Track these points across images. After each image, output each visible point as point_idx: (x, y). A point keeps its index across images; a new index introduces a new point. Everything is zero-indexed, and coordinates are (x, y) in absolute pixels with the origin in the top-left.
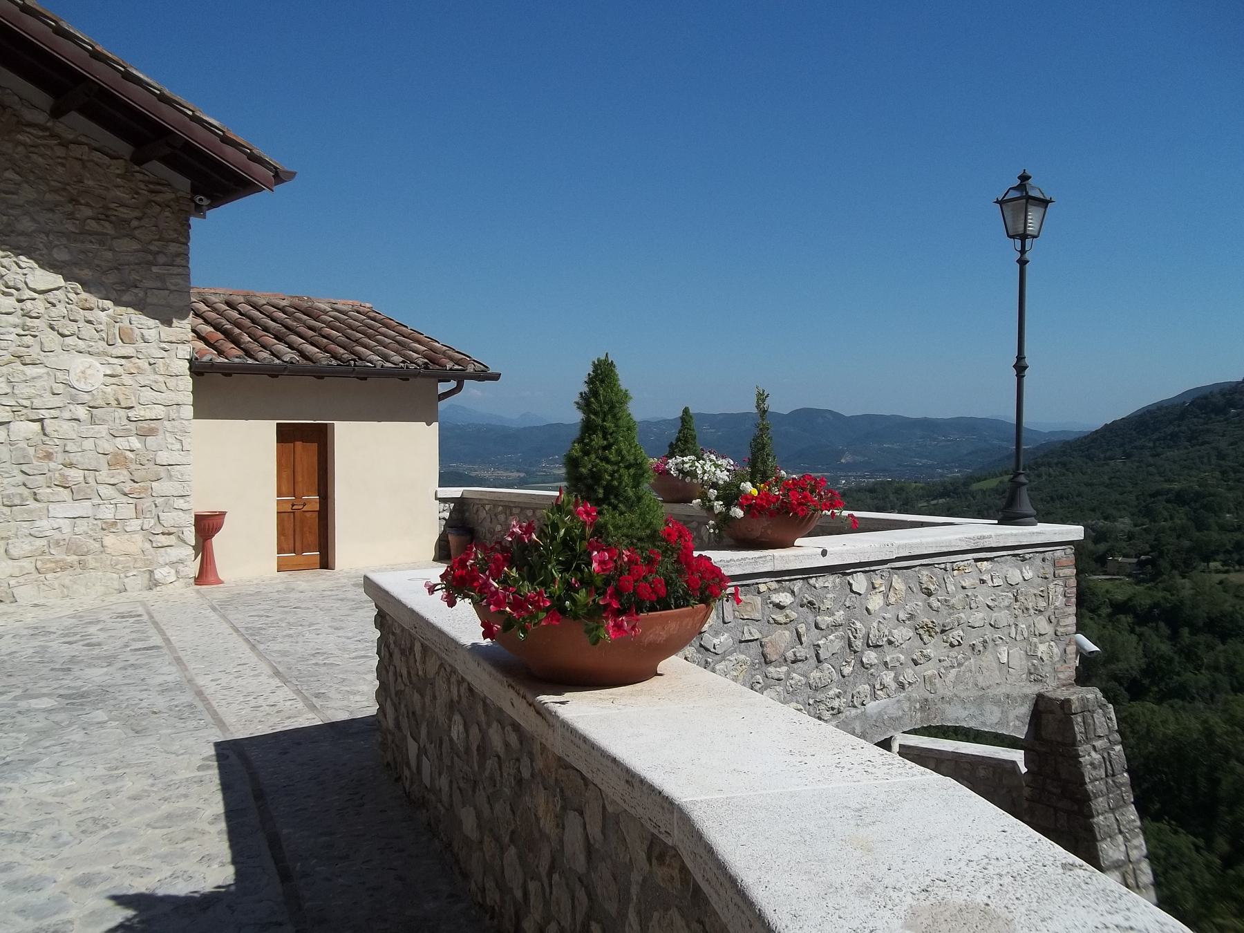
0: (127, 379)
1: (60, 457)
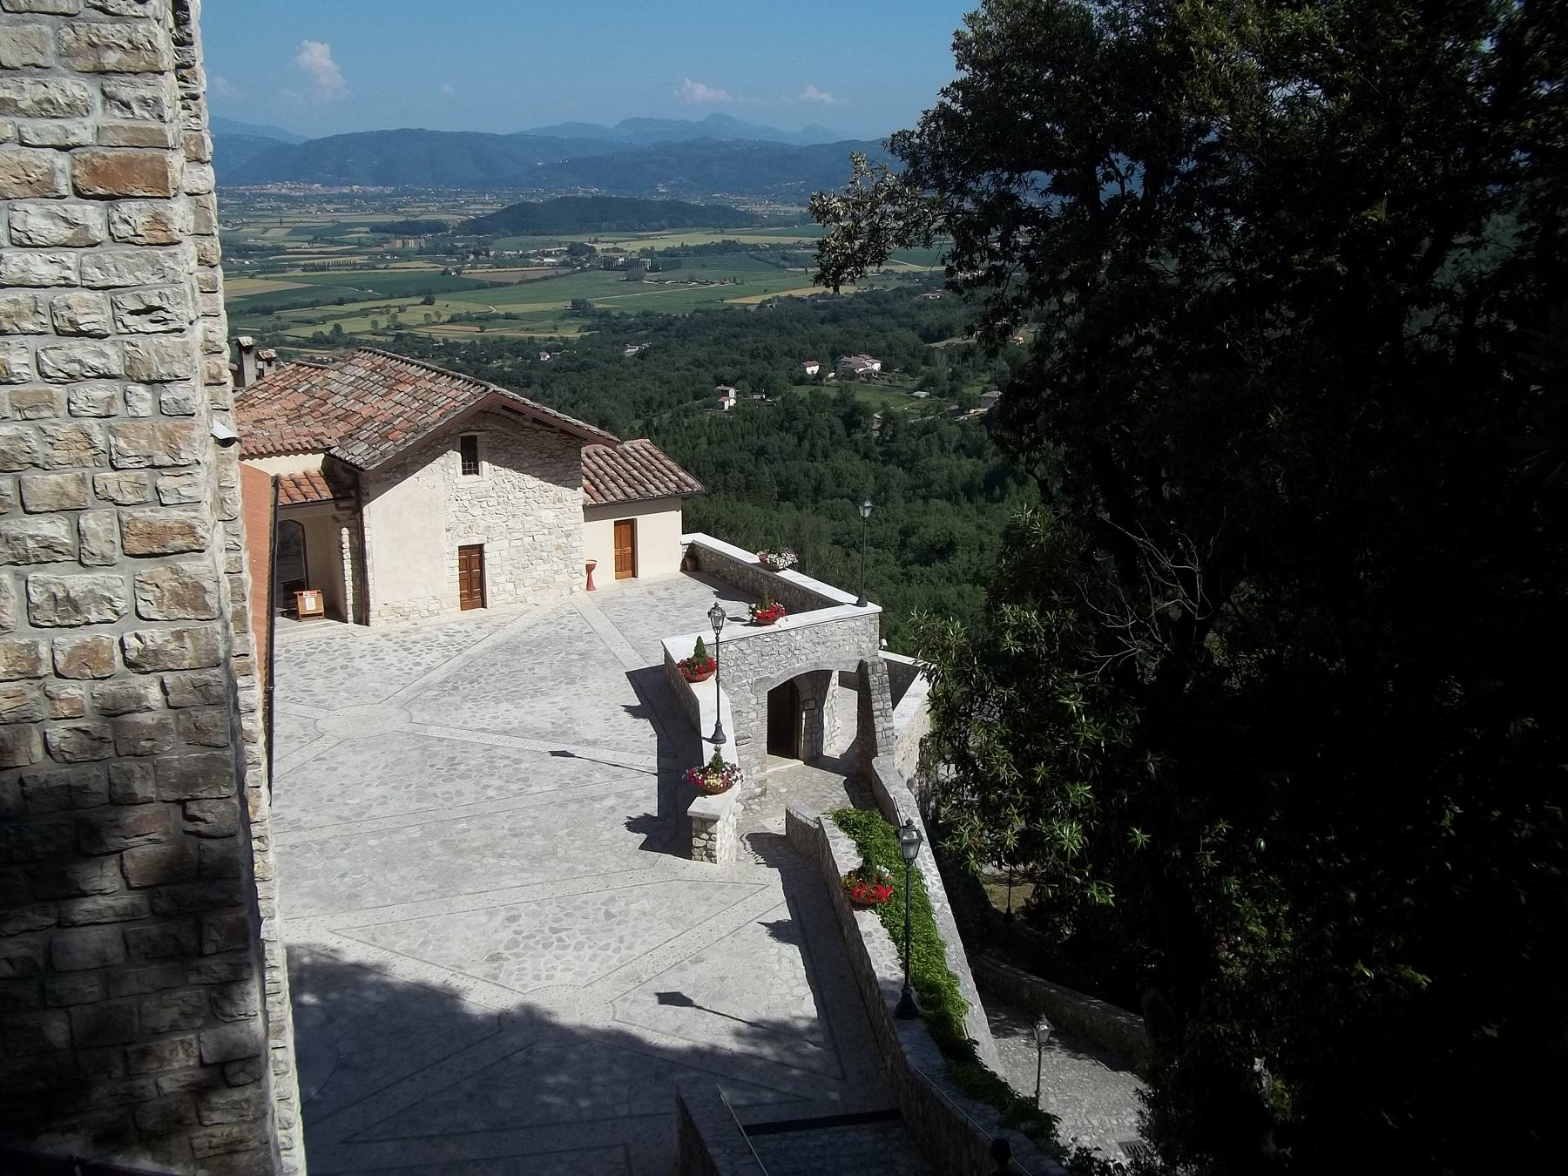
0: (561, 516)
1: (539, 548)
